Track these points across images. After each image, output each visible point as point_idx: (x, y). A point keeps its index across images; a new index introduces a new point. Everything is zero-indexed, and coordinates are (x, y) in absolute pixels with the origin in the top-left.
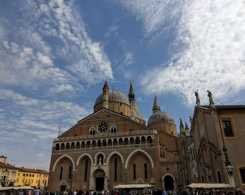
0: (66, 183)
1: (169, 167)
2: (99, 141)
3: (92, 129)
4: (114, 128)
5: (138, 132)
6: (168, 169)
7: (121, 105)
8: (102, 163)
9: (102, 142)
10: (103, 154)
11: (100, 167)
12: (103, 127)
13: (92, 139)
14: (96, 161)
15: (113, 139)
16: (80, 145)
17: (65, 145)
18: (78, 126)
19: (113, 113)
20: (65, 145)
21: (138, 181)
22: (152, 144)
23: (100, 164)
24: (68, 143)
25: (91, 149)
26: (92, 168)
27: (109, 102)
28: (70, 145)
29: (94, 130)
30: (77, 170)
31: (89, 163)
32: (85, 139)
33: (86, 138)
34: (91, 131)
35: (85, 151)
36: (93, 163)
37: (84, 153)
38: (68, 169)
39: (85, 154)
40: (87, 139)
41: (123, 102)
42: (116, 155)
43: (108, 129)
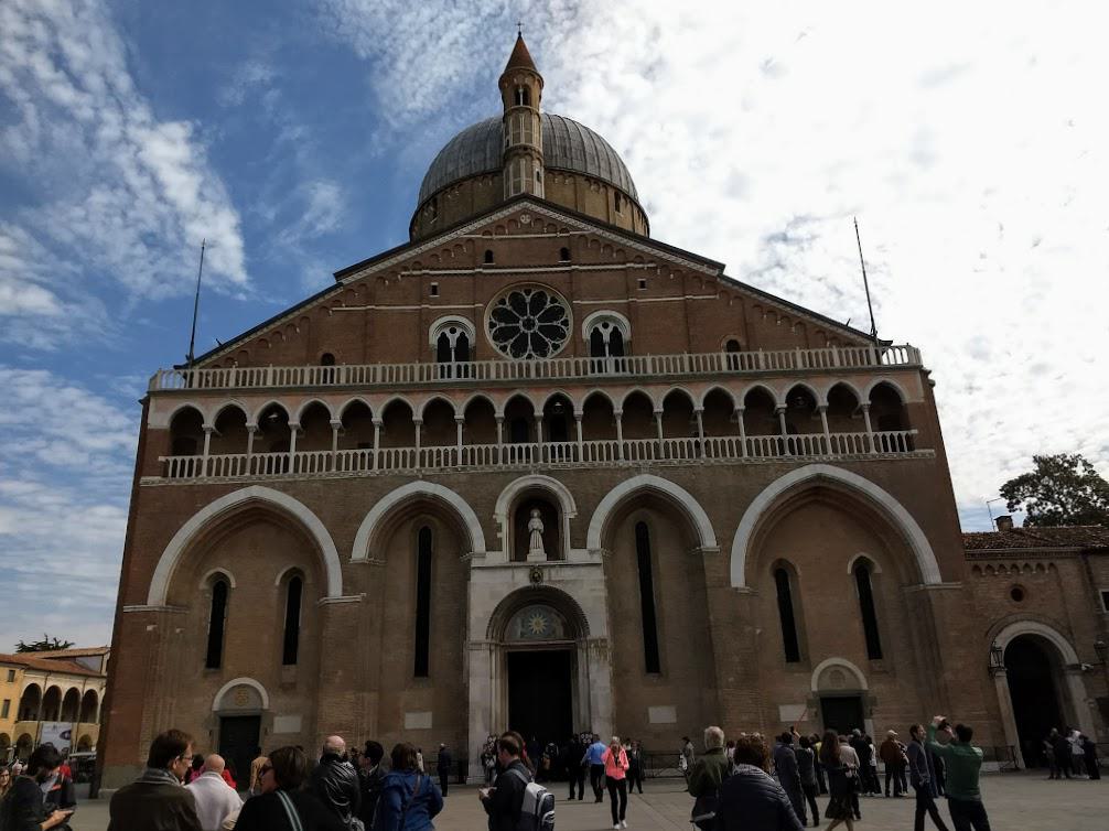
0: (257, 692)
1: (1024, 579)
2: (519, 407)
3: (447, 331)
6: (1017, 594)
7: (617, 208)
8: (553, 549)
9: (539, 412)
10: (556, 486)
11: (546, 578)
12: (529, 324)
13: (462, 391)
14: (504, 534)
15: (623, 398)
18: (337, 302)
20: (252, 422)
23: (537, 554)
25: (465, 456)
26: (477, 578)
27: (549, 170)
29: (463, 340)
30: (358, 598)
32: (412, 389)
33: (417, 379)
36: (487, 550)
39: (420, 482)
40: (429, 388)
42: (647, 499)
43: (563, 336)
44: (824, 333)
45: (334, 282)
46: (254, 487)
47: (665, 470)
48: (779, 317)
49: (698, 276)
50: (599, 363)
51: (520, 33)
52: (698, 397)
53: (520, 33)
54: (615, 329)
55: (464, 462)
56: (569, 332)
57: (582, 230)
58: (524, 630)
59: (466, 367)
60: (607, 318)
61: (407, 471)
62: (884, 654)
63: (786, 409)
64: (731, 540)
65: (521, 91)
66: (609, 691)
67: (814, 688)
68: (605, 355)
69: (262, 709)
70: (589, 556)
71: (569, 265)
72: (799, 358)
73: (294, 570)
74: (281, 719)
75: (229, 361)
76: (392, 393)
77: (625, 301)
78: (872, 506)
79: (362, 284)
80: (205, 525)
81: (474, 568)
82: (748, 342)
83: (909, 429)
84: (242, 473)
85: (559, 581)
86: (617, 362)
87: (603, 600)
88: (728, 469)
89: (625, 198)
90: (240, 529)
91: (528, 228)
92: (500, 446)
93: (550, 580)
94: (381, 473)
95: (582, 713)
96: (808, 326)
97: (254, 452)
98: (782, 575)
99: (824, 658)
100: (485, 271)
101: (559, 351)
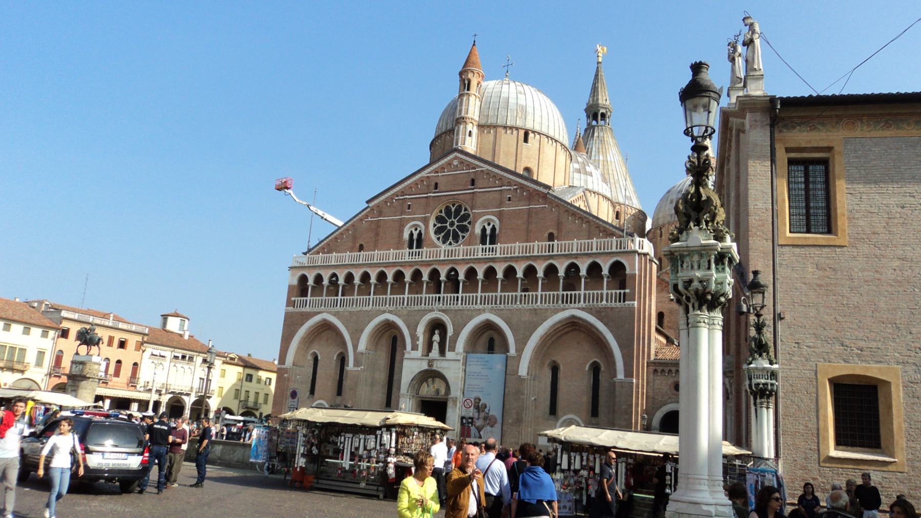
2: (435, 274)
4: (491, 226)
5: (575, 245)
7: (526, 140)
8: (442, 352)
9: (443, 277)
10: (446, 318)
11: (435, 366)
12: (452, 224)
14: (421, 342)
16: (371, 285)
17: (326, 282)
19: (490, 168)
22: (624, 293)
24: (334, 275)
26: (406, 363)
27: (480, 126)
28: (341, 281)
30: (359, 369)
31: (398, 349)
35: (387, 306)
36: (412, 350)
37: (384, 312)
41: (537, 128)
42: (489, 326)
43: (467, 231)
45: (367, 205)
46: (325, 313)
48: (577, 218)
49: (538, 193)
51: (474, 41)
52: (520, 268)
53: (474, 41)
54: (494, 226)
55: (408, 304)
60: (488, 220)
61: (382, 308)
62: (599, 415)
64: (523, 350)
65: (466, 82)
71: (473, 189)
72: (575, 245)
75: (318, 253)
76: (380, 267)
78: (599, 334)
79: (378, 206)
82: (558, 234)
83: (624, 288)
84: (321, 306)
85: (441, 368)
86: (483, 249)
88: (528, 311)
90: (322, 332)
92: (424, 296)
93: (436, 367)
96: (592, 223)
97: (326, 296)
98: (555, 369)
99: (565, 414)
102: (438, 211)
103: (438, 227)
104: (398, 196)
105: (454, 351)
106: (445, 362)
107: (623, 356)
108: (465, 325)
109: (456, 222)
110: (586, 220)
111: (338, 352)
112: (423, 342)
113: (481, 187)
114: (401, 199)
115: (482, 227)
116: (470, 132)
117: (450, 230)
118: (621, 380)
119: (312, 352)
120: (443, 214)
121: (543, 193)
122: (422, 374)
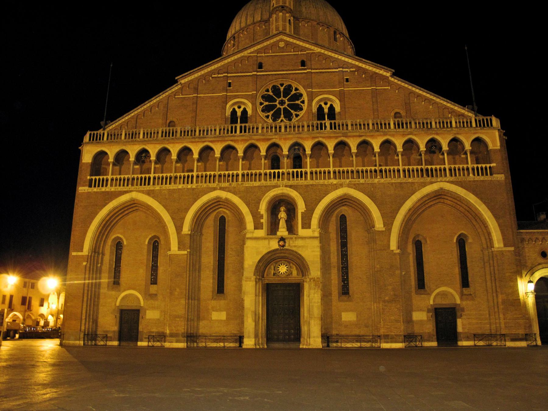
8: (291, 229)
10: (294, 194)
11: (287, 245)
12: (282, 103)
14: (264, 221)
19: (323, 51)
21: (435, 298)
22: (490, 167)
23: (282, 231)
26: (249, 244)
29: (245, 112)
30: (186, 252)
34: (234, 112)
36: (255, 229)
37: (214, 189)
38: (145, 251)
43: (301, 109)
44: (448, 109)
47: (357, 185)
50: (321, 124)
54: (331, 105)
56: (305, 107)
57: (313, 50)
58: (275, 272)
59: (245, 127)
62: (470, 285)
63: (425, 151)
64: (392, 224)
66: (320, 304)
67: (431, 302)
68: (325, 120)
69: (140, 306)
70: (312, 233)
71: (305, 69)
73: (155, 237)
74: (150, 311)
77: (338, 89)
80: (110, 212)
81: (248, 238)
83: (490, 163)
84: (128, 185)
85: (295, 246)
86: (331, 124)
87: (319, 256)
89: (339, 33)
91: (282, 50)
93: (289, 246)
94: (198, 186)
95: (306, 315)
99: (438, 287)
100: (258, 74)
101: (299, 117)
102: (264, 91)
103: (266, 106)
104: (214, 74)
105: (309, 227)
106: (300, 240)
107: (500, 225)
108: (320, 200)
109: (286, 101)
110: (433, 102)
111: (150, 236)
112: (268, 220)
113: (313, 67)
114: (219, 77)
115: (318, 106)
116: (290, 20)
117: (280, 109)
118: (502, 248)
119: (113, 237)
120: (271, 93)
121: (384, 76)
122: (270, 255)
